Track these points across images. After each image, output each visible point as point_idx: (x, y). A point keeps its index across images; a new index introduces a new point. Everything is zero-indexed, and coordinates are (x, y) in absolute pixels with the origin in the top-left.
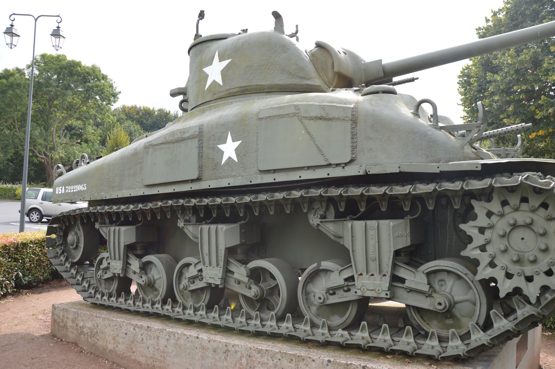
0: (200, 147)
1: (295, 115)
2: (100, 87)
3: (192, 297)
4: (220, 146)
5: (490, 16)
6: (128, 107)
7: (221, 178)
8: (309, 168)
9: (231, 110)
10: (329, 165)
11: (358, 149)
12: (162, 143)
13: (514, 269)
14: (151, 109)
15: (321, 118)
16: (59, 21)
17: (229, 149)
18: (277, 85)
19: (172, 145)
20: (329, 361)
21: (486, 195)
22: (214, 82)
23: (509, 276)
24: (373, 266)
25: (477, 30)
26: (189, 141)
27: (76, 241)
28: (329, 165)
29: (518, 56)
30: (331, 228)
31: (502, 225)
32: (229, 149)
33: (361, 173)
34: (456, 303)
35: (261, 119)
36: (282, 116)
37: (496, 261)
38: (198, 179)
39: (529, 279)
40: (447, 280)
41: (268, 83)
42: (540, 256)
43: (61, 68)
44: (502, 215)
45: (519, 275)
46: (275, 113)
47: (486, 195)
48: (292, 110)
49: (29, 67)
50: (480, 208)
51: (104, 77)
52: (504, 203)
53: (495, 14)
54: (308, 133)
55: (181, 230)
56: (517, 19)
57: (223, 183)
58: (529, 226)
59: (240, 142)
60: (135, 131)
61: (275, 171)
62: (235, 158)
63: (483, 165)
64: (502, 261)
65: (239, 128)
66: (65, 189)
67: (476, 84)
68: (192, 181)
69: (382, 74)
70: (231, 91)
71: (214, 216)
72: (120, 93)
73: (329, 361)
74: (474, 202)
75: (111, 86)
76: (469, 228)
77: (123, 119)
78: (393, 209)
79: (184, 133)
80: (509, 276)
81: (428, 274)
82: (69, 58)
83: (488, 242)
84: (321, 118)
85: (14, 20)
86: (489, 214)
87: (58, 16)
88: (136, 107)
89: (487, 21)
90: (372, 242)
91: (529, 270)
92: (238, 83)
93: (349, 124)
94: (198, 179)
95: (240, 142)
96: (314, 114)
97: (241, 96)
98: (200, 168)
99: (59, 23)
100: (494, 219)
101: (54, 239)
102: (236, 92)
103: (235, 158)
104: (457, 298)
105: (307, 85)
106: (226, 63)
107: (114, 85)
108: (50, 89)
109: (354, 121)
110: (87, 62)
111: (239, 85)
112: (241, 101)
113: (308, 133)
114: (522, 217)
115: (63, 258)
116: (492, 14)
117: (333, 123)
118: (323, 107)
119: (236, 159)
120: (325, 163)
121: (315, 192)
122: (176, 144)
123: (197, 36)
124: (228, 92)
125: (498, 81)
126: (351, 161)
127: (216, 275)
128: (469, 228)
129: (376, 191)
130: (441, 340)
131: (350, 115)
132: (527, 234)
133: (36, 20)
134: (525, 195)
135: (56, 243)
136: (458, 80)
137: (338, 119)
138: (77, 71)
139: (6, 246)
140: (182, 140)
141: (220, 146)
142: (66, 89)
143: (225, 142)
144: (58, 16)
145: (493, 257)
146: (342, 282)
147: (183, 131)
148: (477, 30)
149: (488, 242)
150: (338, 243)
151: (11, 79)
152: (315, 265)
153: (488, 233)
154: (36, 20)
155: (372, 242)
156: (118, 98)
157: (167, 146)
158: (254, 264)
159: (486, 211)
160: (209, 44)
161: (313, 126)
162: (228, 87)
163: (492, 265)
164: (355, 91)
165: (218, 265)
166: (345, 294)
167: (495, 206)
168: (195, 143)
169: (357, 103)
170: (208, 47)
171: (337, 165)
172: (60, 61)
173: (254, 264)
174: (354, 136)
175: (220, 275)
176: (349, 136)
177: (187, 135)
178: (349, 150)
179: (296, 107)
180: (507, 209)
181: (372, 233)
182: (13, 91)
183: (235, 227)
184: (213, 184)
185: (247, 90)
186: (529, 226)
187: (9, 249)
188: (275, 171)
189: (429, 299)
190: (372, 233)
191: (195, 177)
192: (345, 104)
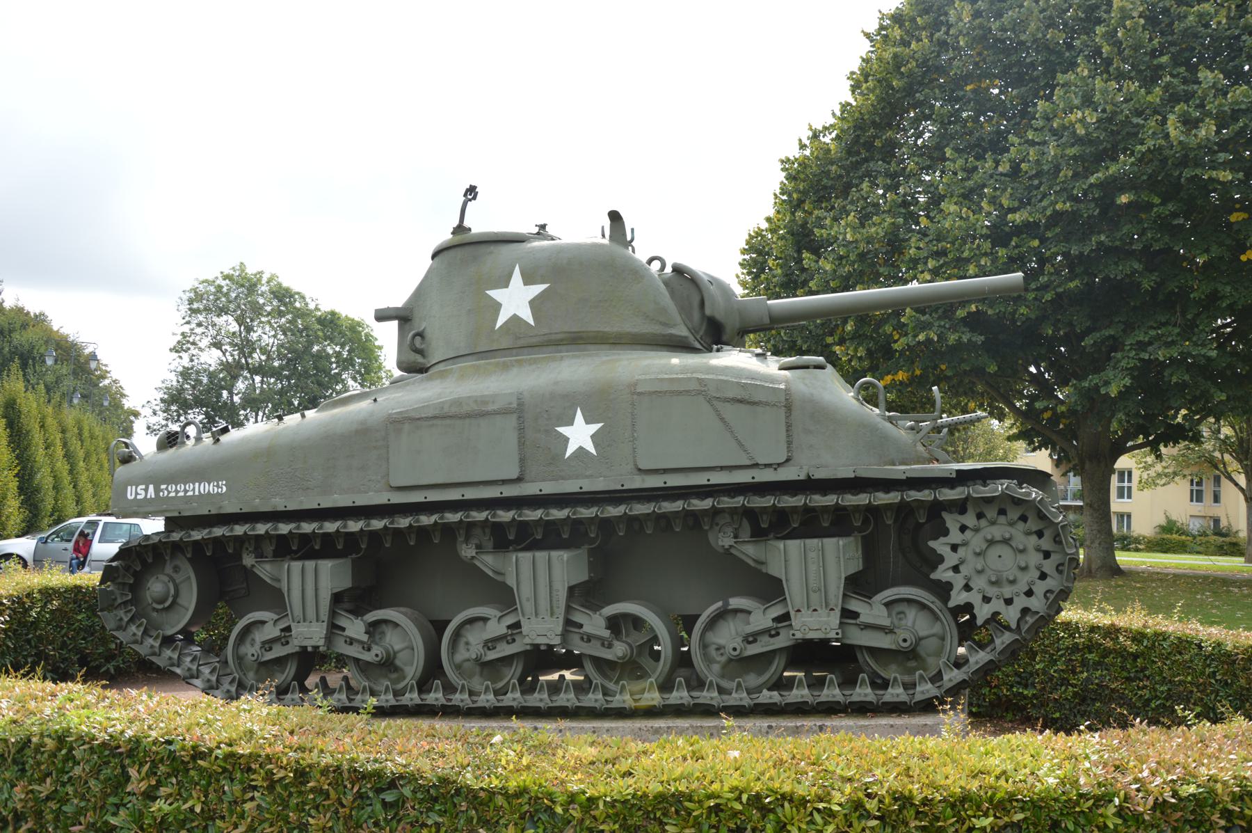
0: (521, 430)
1: (699, 393)
3: (481, 675)
4: (561, 429)
5: (805, 135)
7: (563, 478)
8: (722, 468)
9: (574, 370)
10: (756, 465)
11: (794, 446)
12: (435, 417)
13: (991, 591)
15: (741, 401)
17: (580, 434)
18: (628, 333)
20: (770, 727)
21: (960, 507)
23: (987, 600)
25: (782, 162)
27: (172, 592)
28: (756, 465)
29: (863, 226)
30: (488, 562)
31: (977, 542)
32: (580, 434)
33: (802, 478)
34: (921, 639)
35: (640, 394)
36: (679, 393)
37: (971, 584)
38: (519, 480)
39: (1009, 602)
40: (907, 612)
41: (615, 329)
42: (1019, 575)
44: (977, 530)
45: (998, 597)
47: (960, 507)
48: (693, 386)
50: (952, 521)
52: (980, 516)
53: (815, 136)
54: (722, 419)
55: (249, 574)
56: (859, 153)
57: (570, 487)
58: (1006, 541)
59: (600, 425)
61: (665, 471)
62: (591, 449)
63: (958, 471)
64: (979, 583)
65: (596, 403)
66: (157, 490)
67: (779, 271)
68: (504, 482)
69: (767, 320)
70: (553, 337)
73: (770, 727)
74: (945, 515)
76: (940, 546)
78: (839, 522)
79: (485, 403)
80: (987, 600)
81: (888, 605)
83: (962, 562)
84: (741, 401)
86: (963, 529)
89: (803, 147)
91: (1007, 591)
92: (563, 326)
93: (783, 410)
94: (519, 480)
95: (600, 425)
96: (730, 395)
97: (569, 347)
98: (522, 461)
100: (968, 533)
102: (562, 340)
103: (591, 449)
104: (922, 634)
105: (671, 335)
106: (538, 289)
109: (789, 407)
111: (566, 329)
112: (578, 357)
113: (722, 419)
114: (997, 532)
116: (810, 134)
117: (759, 409)
118: (744, 386)
120: (748, 463)
121: (727, 502)
122: (467, 421)
123: (460, 229)
124: (546, 338)
125: (826, 272)
126: (788, 460)
127: (550, 630)
128: (940, 546)
130: (906, 686)
131: (783, 399)
132: (1005, 551)
134: (1003, 506)
135: (115, 599)
136: (740, 258)
137: (767, 404)
141: (561, 429)
143: (570, 422)
145: (968, 579)
146: (769, 624)
147: (483, 400)
148: (782, 162)
149: (962, 562)
150: (760, 571)
152: (720, 604)
153: (961, 551)
157: (448, 422)
158: (611, 610)
159: (958, 526)
160: (492, 248)
161: (729, 411)
162: (546, 331)
163: (967, 588)
164: (758, 355)
166: (772, 640)
167: (970, 519)
168: (512, 421)
169: (787, 382)
170: (491, 253)
171: (767, 466)
173: (611, 610)
174: (789, 427)
175: (559, 629)
176: (783, 429)
177: (490, 408)
178: (784, 446)
180: (983, 522)
181: (812, 555)
183: (582, 553)
184: (549, 488)
185: (581, 338)
186: (1006, 541)
188: (665, 471)
189: (889, 637)
191: (515, 476)
192: (772, 382)
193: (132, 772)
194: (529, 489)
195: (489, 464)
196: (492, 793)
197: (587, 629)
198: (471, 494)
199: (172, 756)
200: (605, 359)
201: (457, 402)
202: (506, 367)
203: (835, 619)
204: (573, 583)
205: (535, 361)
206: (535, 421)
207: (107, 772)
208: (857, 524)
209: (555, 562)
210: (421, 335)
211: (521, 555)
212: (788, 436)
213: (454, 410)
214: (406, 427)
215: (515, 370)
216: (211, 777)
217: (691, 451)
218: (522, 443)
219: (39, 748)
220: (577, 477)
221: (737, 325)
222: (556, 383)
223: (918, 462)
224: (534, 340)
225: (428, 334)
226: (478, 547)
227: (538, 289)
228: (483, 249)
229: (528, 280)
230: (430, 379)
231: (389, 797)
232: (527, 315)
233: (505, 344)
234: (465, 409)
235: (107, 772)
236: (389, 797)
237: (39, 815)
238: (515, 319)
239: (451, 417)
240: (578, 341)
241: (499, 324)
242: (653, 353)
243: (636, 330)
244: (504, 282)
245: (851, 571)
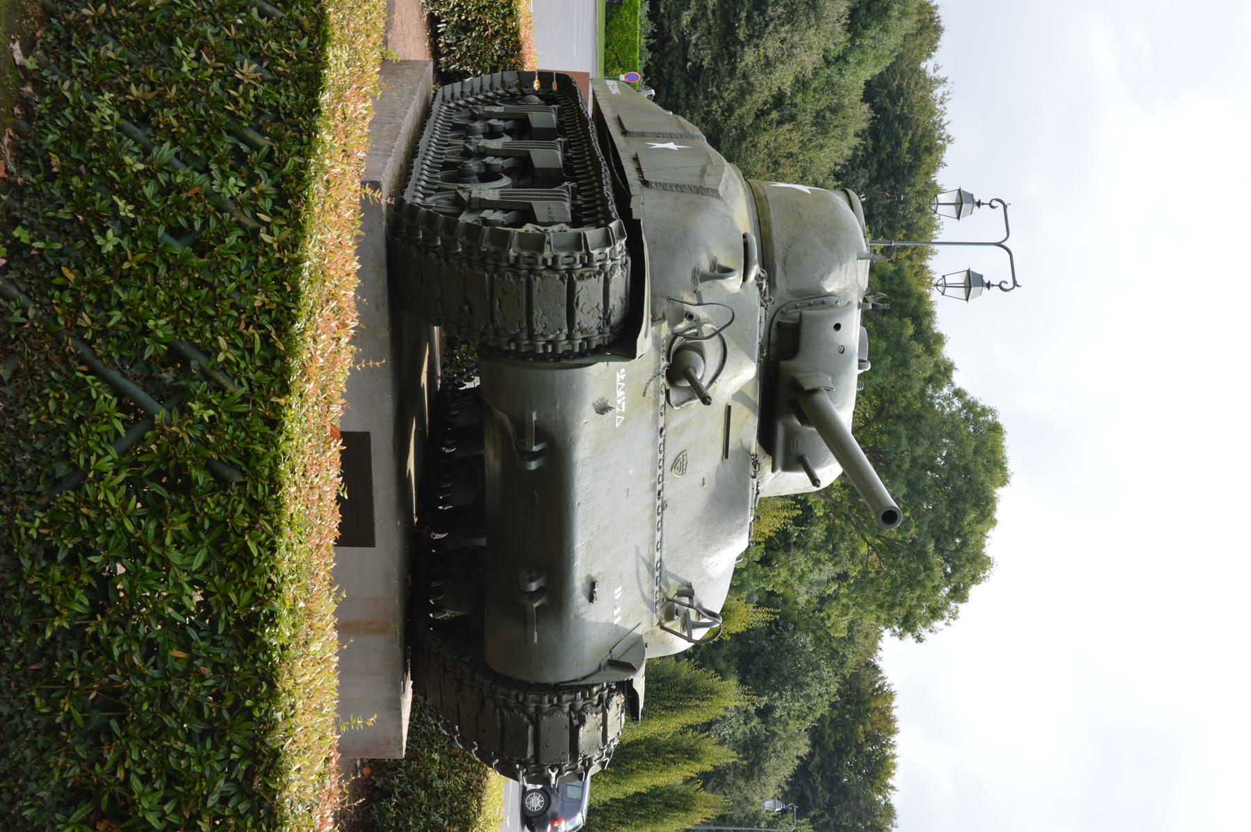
2: (928, 577)
6: (888, 709)
14: (890, 781)
16: (1004, 286)
18: (770, 230)
38: (625, 133)
43: (966, 470)
49: (959, 394)
51: (959, 594)
60: (808, 697)
69: (807, 387)
72: (919, 639)
75: (935, 613)
77: (842, 664)
82: (1001, 493)
85: (992, 207)
87: (1015, 284)
88: (892, 732)
93: (695, 181)
99: (1000, 286)
101: (532, 85)
107: (938, 624)
108: (904, 442)
109: (700, 190)
110: (995, 543)
115: (501, 92)
126: (645, 183)
133: (999, 244)
138: (965, 512)
139: (520, 49)
142: (909, 484)
144: (1015, 284)
151: (919, 348)
154: (999, 244)
156: (901, 636)
172: (988, 470)
174: (680, 188)
182: (887, 352)
187: (512, 56)
212: (671, 186)
221: (799, 376)
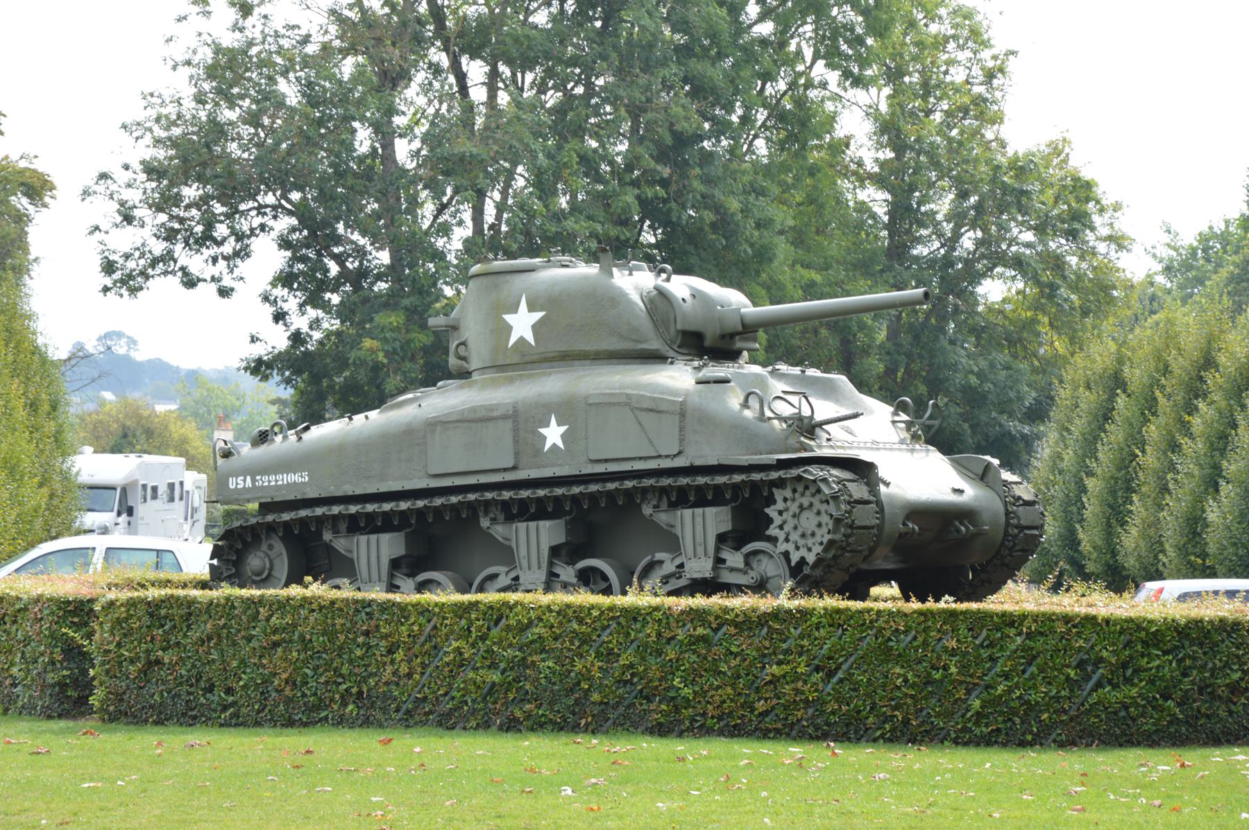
0: (516, 430)
1: (626, 404)
4: (541, 430)
9: (552, 384)
12: (458, 421)
15: (651, 410)
19: (474, 425)
22: (522, 339)
24: (700, 550)
26: (500, 422)
31: (794, 508)
35: (590, 405)
36: (614, 404)
42: (817, 530)
44: (793, 500)
46: (607, 400)
48: (623, 399)
57: (547, 473)
65: (566, 410)
68: (505, 470)
71: (532, 511)
74: (774, 490)
78: (714, 497)
79: (492, 410)
84: (651, 410)
90: (699, 528)
94: (514, 468)
96: (645, 406)
103: (561, 445)
106: (538, 315)
114: (805, 501)
118: (654, 399)
119: (562, 446)
129: (701, 480)
137: (668, 412)
140: (490, 419)
141: (541, 430)
147: (490, 408)
149: (785, 522)
150: (671, 533)
153: (785, 515)
155: (699, 528)
158: (581, 564)
162: (542, 350)
165: (539, 568)
167: (788, 493)
168: (509, 425)
173: (581, 564)
175: (543, 578)
178: (677, 443)
179: (627, 395)
181: (699, 520)
184: (534, 474)
190: (699, 520)
193: (261, 610)
194: (521, 475)
195: (491, 458)
196: (407, 605)
197: (562, 578)
198: (484, 479)
199: (279, 601)
200: (581, 373)
201: (474, 409)
202: (511, 380)
203: (709, 564)
204: (553, 544)
205: (532, 376)
206: (523, 422)
207: (249, 612)
208: (728, 496)
209: (542, 531)
210: (463, 344)
211: (519, 524)
213: (471, 416)
214: (439, 429)
215: (517, 383)
216: (295, 608)
217: (623, 447)
218: (516, 441)
219: (218, 605)
220: (553, 465)
222: (540, 395)
223: (786, 452)
224: (535, 357)
225: (470, 343)
226: (492, 519)
227: (538, 315)
228: (502, 278)
229: (532, 308)
230: (470, 386)
231: (368, 610)
232: (530, 338)
233: (515, 359)
234: (479, 415)
235: (249, 612)
236: (368, 610)
237: (219, 636)
238: (522, 340)
239: (468, 421)
240: (567, 358)
241: (511, 343)
242: (620, 367)
243: (612, 348)
244: (514, 309)
245: (722, 530)
